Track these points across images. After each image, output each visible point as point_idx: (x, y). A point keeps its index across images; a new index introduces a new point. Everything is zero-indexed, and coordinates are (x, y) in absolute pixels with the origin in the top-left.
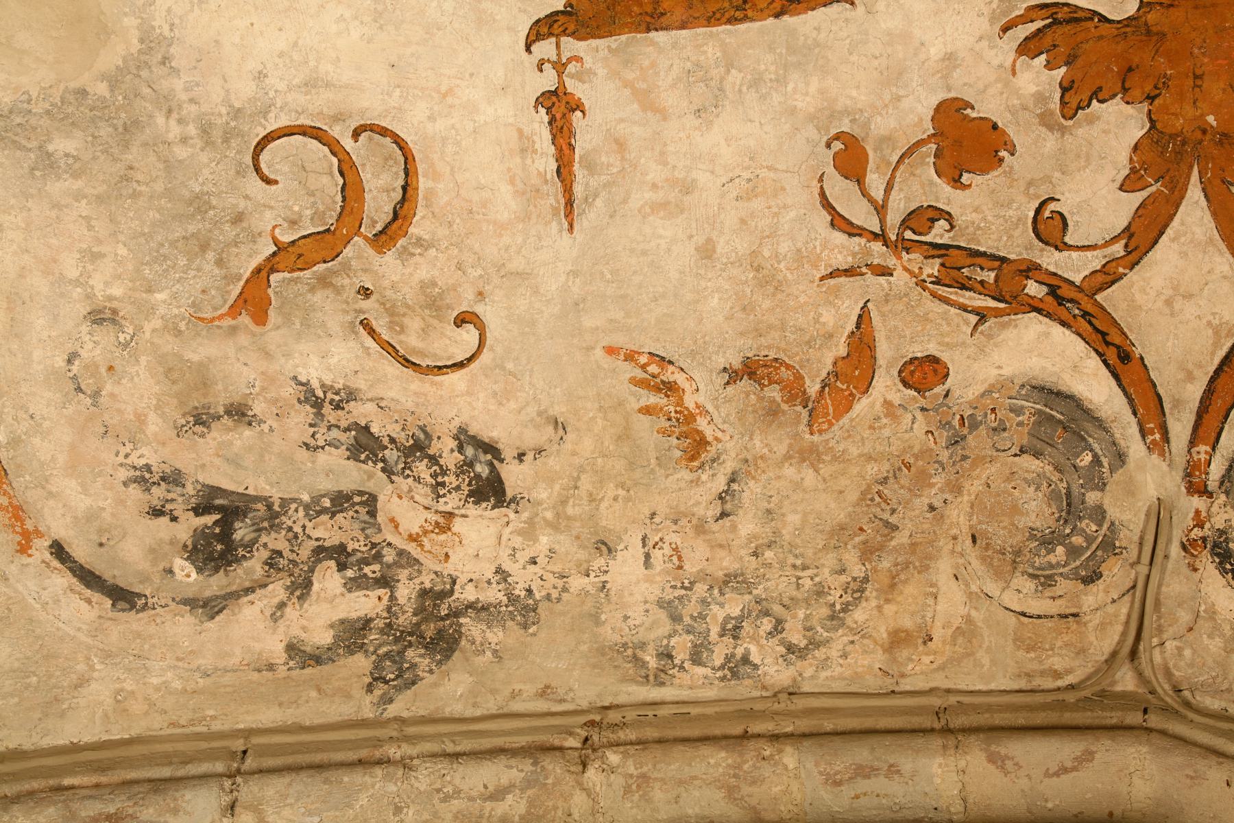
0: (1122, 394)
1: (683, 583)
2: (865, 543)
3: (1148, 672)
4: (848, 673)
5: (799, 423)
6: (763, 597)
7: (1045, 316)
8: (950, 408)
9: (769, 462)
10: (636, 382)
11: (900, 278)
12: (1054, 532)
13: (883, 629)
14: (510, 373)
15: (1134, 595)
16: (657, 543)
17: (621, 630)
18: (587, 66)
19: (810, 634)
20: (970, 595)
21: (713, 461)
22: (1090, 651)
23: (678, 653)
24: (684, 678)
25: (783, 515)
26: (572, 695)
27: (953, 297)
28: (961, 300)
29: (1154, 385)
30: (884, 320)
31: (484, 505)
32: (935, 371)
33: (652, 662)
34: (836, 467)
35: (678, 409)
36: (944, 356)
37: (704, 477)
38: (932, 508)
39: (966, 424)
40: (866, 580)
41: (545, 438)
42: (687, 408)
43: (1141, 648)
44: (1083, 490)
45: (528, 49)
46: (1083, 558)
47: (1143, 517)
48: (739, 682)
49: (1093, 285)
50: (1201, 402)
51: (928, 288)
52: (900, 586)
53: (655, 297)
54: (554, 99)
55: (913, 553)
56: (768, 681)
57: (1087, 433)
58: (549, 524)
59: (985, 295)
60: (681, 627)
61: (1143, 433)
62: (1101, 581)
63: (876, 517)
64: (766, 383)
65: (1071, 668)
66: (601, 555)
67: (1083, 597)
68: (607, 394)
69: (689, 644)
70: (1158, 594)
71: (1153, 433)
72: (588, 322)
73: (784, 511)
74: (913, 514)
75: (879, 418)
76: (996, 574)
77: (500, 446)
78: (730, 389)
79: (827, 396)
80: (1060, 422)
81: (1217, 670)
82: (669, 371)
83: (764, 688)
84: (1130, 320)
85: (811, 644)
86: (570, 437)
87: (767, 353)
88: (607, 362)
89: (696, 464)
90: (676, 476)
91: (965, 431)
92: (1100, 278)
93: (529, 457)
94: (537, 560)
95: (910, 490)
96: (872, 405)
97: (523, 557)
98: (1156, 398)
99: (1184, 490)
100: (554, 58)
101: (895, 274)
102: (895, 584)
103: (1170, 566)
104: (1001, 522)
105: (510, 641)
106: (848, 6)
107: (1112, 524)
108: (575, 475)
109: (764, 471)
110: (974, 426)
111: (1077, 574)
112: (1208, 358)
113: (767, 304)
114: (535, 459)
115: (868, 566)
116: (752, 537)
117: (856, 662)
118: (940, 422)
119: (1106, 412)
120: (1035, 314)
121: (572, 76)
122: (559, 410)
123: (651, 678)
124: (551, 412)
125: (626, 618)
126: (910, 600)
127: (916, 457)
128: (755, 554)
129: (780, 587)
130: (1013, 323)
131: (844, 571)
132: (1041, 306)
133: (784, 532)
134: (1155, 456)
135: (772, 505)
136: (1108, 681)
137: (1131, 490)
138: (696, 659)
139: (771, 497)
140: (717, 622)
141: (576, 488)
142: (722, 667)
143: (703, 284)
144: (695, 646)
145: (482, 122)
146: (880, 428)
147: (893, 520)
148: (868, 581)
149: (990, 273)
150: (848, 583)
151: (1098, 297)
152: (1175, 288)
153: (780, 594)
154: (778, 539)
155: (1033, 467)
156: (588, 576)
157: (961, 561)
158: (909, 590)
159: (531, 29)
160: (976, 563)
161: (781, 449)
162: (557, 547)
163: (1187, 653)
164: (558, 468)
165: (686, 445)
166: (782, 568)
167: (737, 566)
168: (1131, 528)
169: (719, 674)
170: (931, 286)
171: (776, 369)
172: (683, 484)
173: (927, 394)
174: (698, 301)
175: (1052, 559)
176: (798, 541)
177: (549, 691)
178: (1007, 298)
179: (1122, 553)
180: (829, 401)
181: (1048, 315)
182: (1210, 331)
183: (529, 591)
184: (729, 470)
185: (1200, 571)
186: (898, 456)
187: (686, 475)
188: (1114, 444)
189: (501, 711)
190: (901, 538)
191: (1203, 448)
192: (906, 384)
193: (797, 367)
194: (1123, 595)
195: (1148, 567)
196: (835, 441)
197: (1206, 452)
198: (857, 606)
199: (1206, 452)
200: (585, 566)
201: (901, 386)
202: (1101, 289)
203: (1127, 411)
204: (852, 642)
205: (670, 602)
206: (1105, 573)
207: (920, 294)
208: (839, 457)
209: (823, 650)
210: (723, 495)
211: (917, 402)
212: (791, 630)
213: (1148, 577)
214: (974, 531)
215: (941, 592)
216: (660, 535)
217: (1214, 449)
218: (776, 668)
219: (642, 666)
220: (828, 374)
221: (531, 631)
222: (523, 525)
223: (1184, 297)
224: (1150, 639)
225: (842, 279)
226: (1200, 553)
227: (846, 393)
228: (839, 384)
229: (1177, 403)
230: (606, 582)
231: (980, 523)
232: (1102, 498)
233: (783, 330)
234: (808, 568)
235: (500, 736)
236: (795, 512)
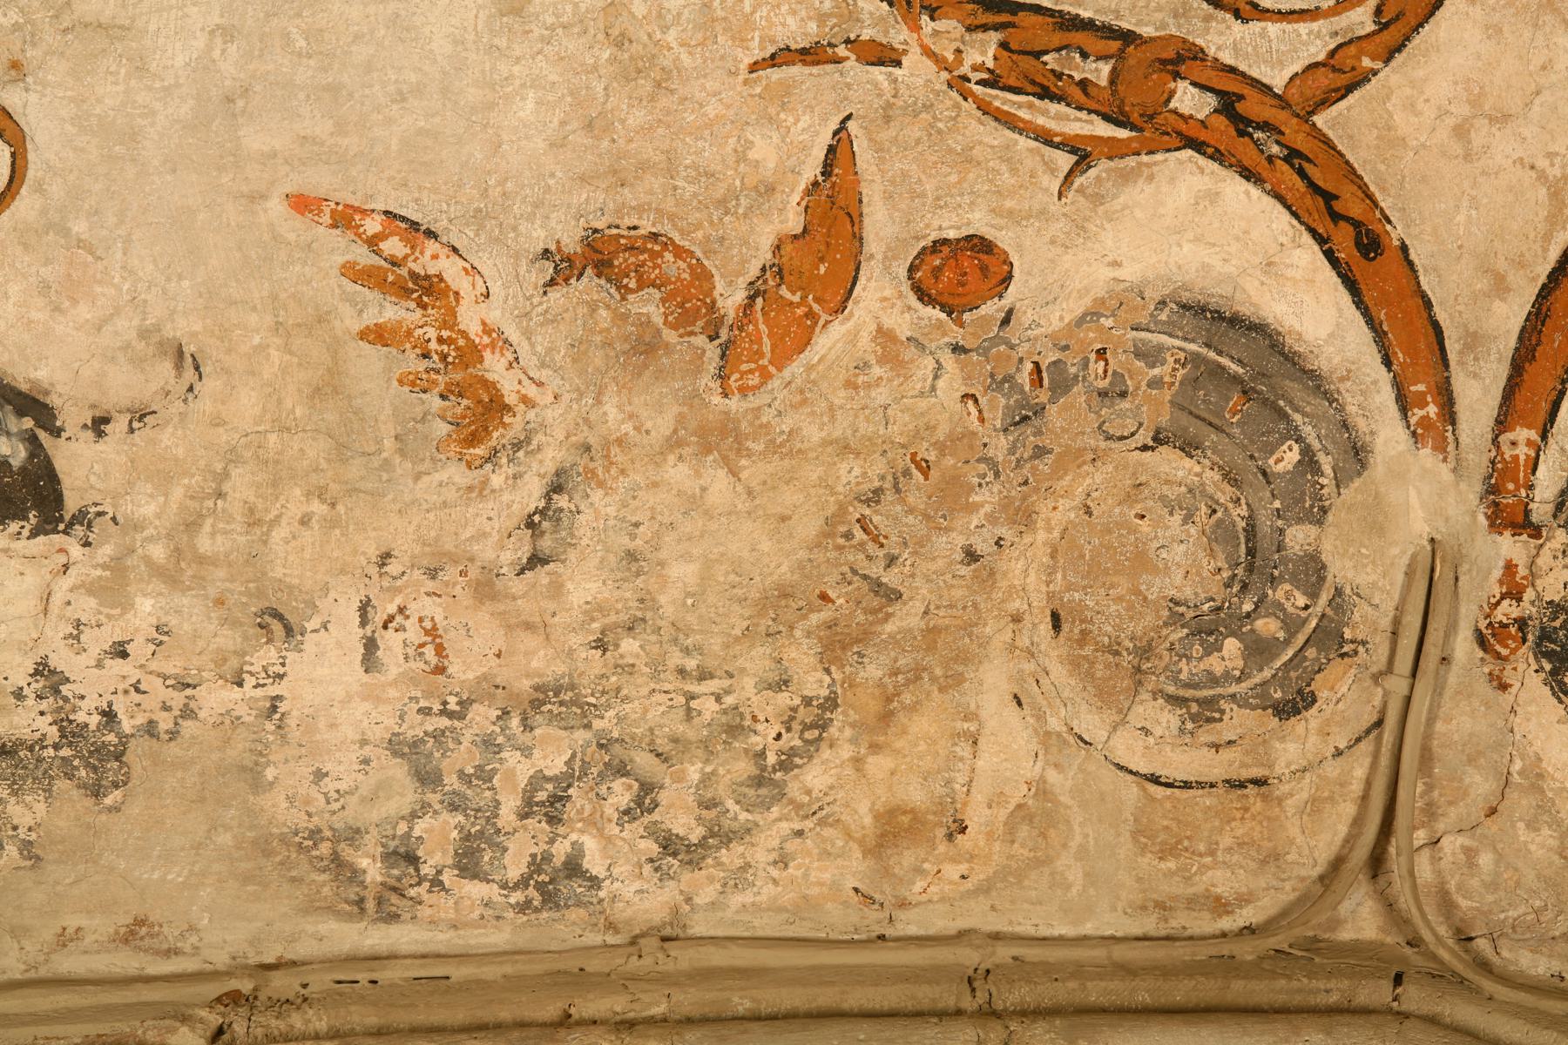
0: (1361, 321)
1: (445, 703)
2: (830, 625)
3: (1405, 901)
4: (788, 897)
5: (698, 371)
6: (615, 734)
7: (1211, 157)
8: (1012, 347)
9: (636, 451)
10: (353, 273)
11: (916, 71)
12: (1219, 609)
13: (864, 808)
14: (81, 244)
15: (1379, 739)
16: (391, 618)
17: (308, 800)
19: (713, 813)
20: (1046, 737)
21: (517, 446)
22: (1289, 858)
23: (430, 853)
24: (443, 906)
25: (662, 564)
26: (194, 939)
27: (1024, 114)
28: (1041, 121)
29: (1428, 305)
30: (882, 160)
31: (14, 526)
32: (984, 269)
33: (373, 870)
34: (775, 465)
35: (445, 334)
36: (1004, 239)
37: (497, 480)
38: (971, 556)
39: (1046, 382)
40: (831, 703)
41: (154, 386)
42: (464, 334)
43: (1392, 850)
44: (1280, 523)
46: (1278, 663)
47: (1400, 578)
48: (557, 915)
49: (1309, 93)
50: (1520, 339)
51: (973, 94)
52: (902, 717)
53: (400, 92)
55: (931, 648)
56: (620, 912)
57: (1290, 402)
58: (157, 571)
59: (1090, 112)
60: (438, 796)
61: (1404, 404)
62: (1313, 711)
63: (854, 572)
64: (632, 285)
65: (1251, 893)
66: (269, 641)
67: (1277, 745)
68: (293, 296)
69: (455, 834)
70: (1428, 736)
71: (1423, 405)
72: (254, 140)
73: (663, 555)
74: (933, 567)
75: (866, 364)
76: (1100, 694)
77: (54, 401)
78: (555, 294)
79: (759, 315)
80: (1236, 379)
81: (1544, 895)
82: (428, 253)
83: (611, 926)
84: (1382, 167)
85: (713, 835)
86: (210, 385)
87: (636, 222)
88: (294, 227)
89: (480, 451)
90: (437, 477)
91: (1043, 396)
92: (1325, 79)
93: (118, 427)
94: (129, 648)
95: (927, 517)
96: (853, 337)
97: (97, 641)
98: (1430, 329)
99: (1483, 521)
101: (905, 61)
102: (891, 713)
103: (1453, 678)
104: (1112, 586)
105: (61, 824)
107: (1339, 592)
108: (219, 467)
109: (623, 472)
110: (1062, 386)
111: (1264, 696)
112: (1537, 247)
113: (637, 117)
114: (132, 431)
115: (837, 675)
116: (595, 609)
117: (806, 876)
118: (992, 376)
119: (1330, 360)
120: (1189, 152)
122: (185, 328)
123: (370, 905)
124: (169, 332)
125: (320, 775)
126: (922, 747)
127: (942, 448)
128: (601, 645)
129: (649, 716)
130: (1146, 171)
131: (786, 683)
132: (1203, 136)
133: (662, 599)
134: (1426, 452)
135: (639, 542)
136: (1323, 918)
137: (1377, 523)
138: (468, 866)
139: (637, 525)
140: (515, 786)
141: (220, 495)
142: (523, 883)
143: (503, 68)
144: (468, 837)
146: (868, 386)
147: (890, 578)
148: (836, 706)
149: (1101, 64)
150: (794, 709)
151: (1319, 120)
152: (1475, 102)
153: (651, 730)
154: (649, 615)
155: (1180, 474)
156: (240, 684)
157: (1029, 667)
158: (921, 725)
160: (1058, 672)
161: (662, 425)
162: (173, 621)
163: (1485, 860)
164: (180, 452)
165: (459, 410)
166: (655, 675)
167: (560, 668)
168: (1376, 601)
169: (517, 897)
170: (978, 89)
171: (655, 255)
172: (451, 495)
173: (966, 316)
174: (491, 106)
175: (1215, 664)
176: (691, 619)
177: (144, 930)
178: (1135, 117)
179: (1356, 652)
180: (762, 327)
181: (1217, 156)
182: (1543, 191)
183: (109, 715)
184: (550, 467)
185: (1514, 690)
186: (903, 446)
187: (456, 474)
188: (1345, 425)
189: (32, 975)
190: (907, 618)
191: (1523, 434)
192: (923, 295)
193: (699, 254)
194: (1358, 740)
195: (1410, 681)
196: (773, 412)
197: (1529, 443)
198: (811, 758)
199: (1529, 443)
200: (234, 662)
201: (912, 299)
202: (1325, 102)
203: (1373, 358)
204: (800, 833)
205: (416, 744)
206: (1323, 695)
207: (957, 106)
208: (782, 445)
209: (738, 848)
210: (537, 518)
211: (945, 334)
212: (671, 806)
213: (1408, 700)
214: (1056, 604)
215: (986, 731)
216: (398, 601)
217: (1544, 437)
218: (637, 885)
219: (351, 880)
220: (763, 269)
221: (108, 801)
222: (99, 572)
223: (1492, 120)
224: (1411, 834)
225: (796, 71)
226: (1514, 651)
227: (800, 312)
228: (784, 292)
229: (1473, 341)
230: (278, 698)
231: (1070, 587)
232: (1318, 538)
233: (671, 173)
234: (712, 677)
235: (24, 1024)
236: (686, 557)
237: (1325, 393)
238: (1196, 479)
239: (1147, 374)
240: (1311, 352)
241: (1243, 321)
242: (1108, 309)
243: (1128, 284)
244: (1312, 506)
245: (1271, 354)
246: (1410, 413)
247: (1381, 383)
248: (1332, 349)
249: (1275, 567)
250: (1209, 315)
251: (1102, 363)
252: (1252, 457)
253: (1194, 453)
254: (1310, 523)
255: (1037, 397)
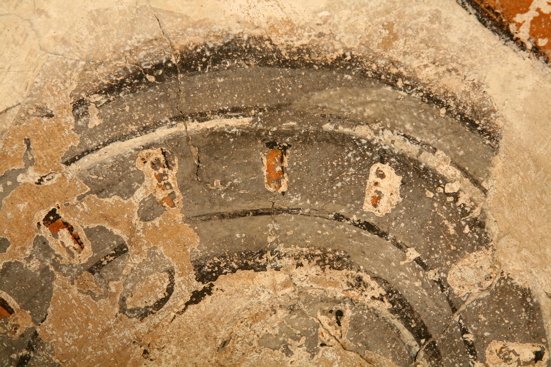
39: (12, 302)
44: (432, 275)
57: (339, 118)
119: (352, 29)
155: (264, 297)
237: (377, 76)
238: (288, 290)
239: (131, 205)
240: (321, 35)
241: (200, 55)
242: (14, 161)
243: (16, 111)
244: (459, 229)
245: (269, 74)
246: (512, 28)
247: (444, 13)
248: (346, 13)
249: (465, 331)
250: (152, 79)
251: (64, 232)
252: (338, 218)
253: (263, 262)
254: (472, 250)
255: (16, 327)
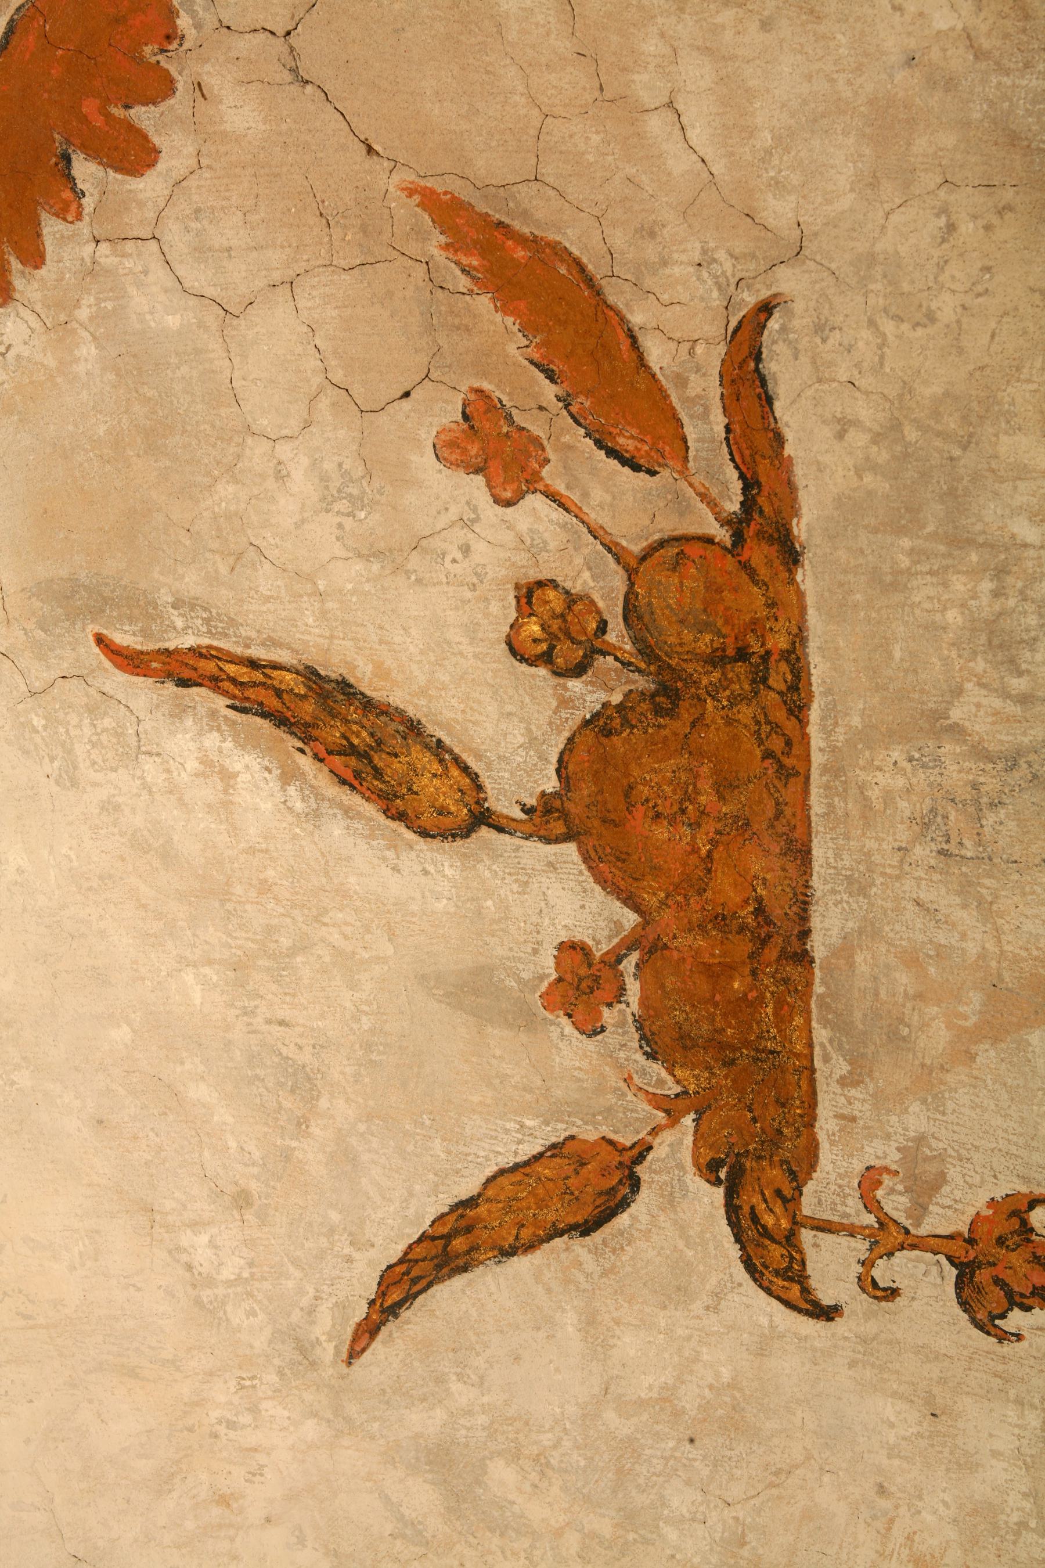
18: (892, 1158)
45: (827, 1313)
54: (983, 1276)
100: (860, 1247)
106: (774, 324)
121: (919, 1210)
145: (1028, 1505)
159: (769, 1292)
